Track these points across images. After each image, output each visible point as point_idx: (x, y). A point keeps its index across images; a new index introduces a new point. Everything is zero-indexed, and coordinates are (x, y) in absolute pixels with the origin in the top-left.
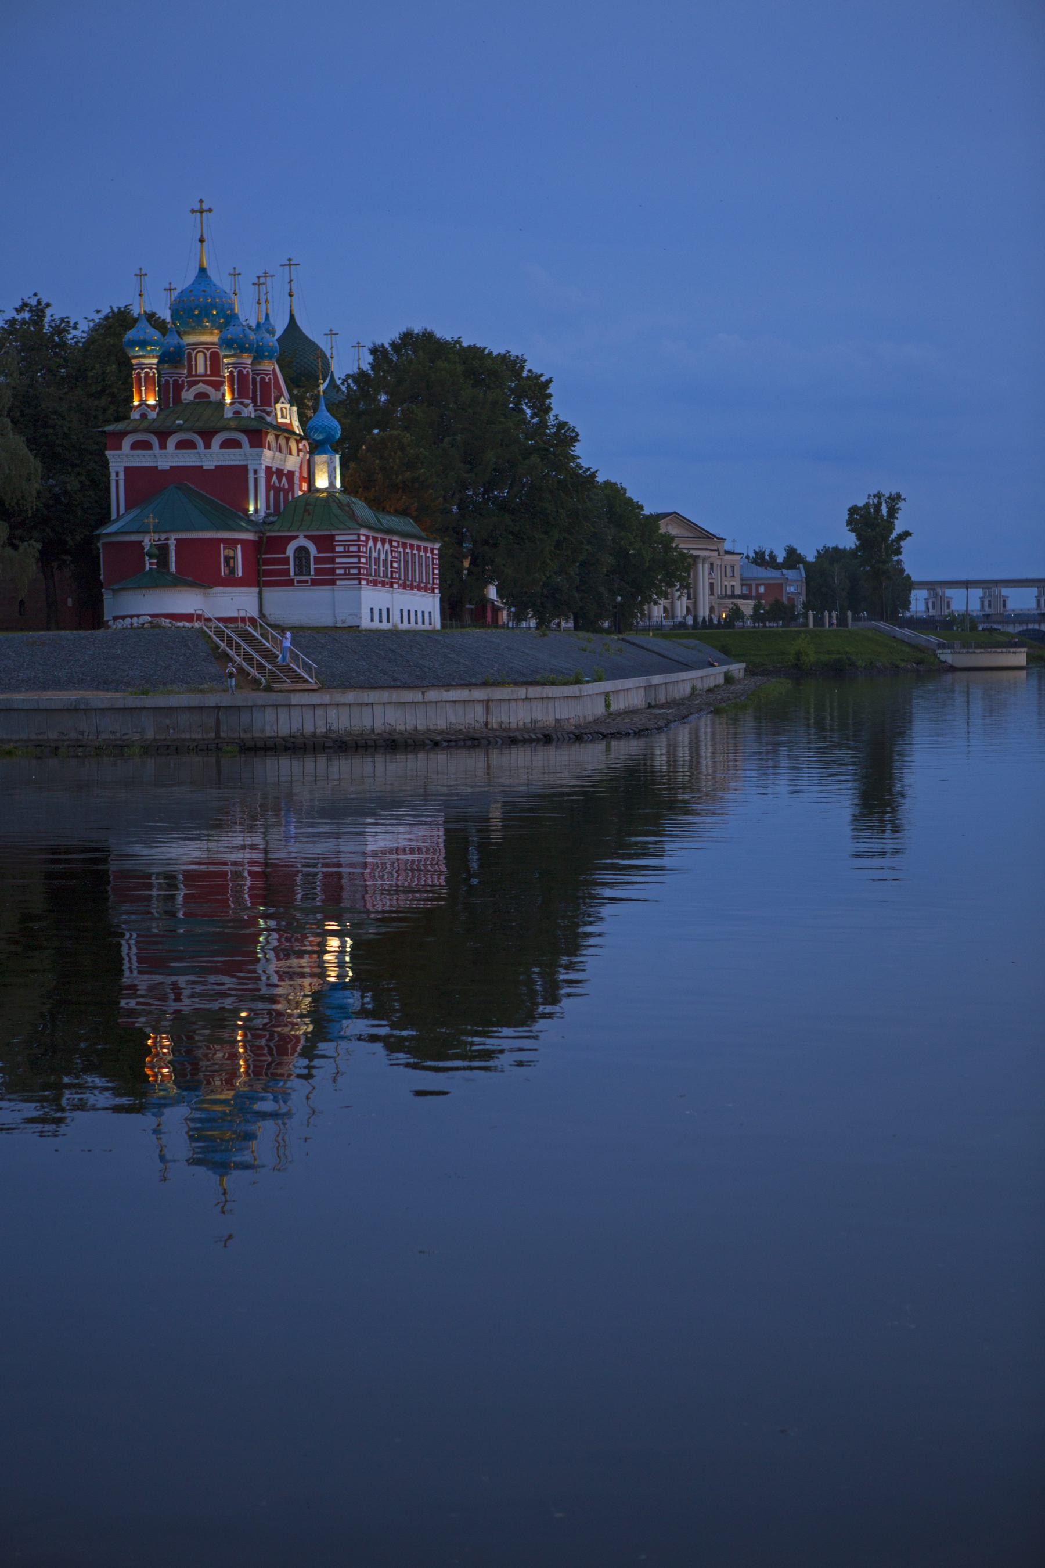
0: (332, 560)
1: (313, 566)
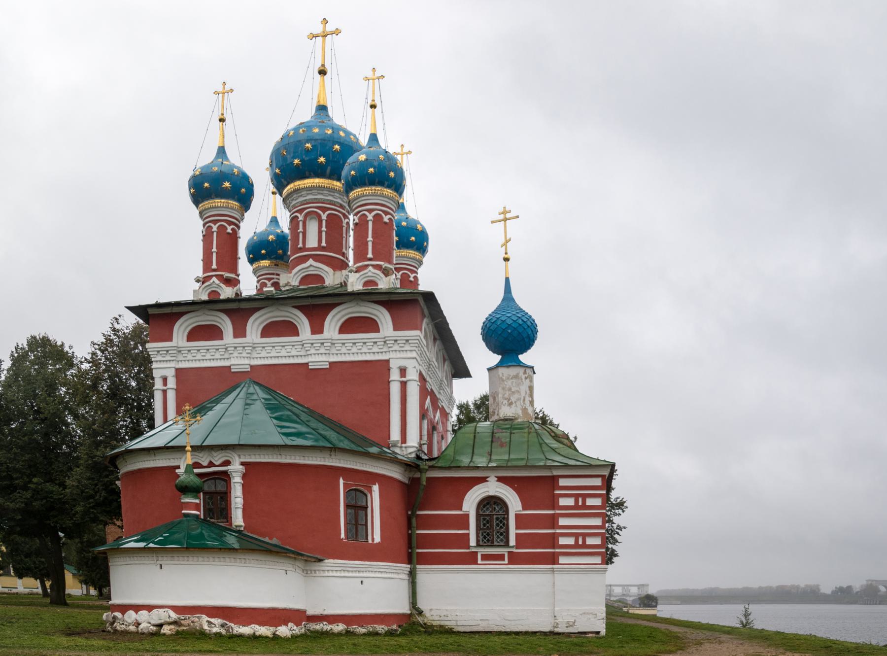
0: (552, 522)
1: (513, 531)
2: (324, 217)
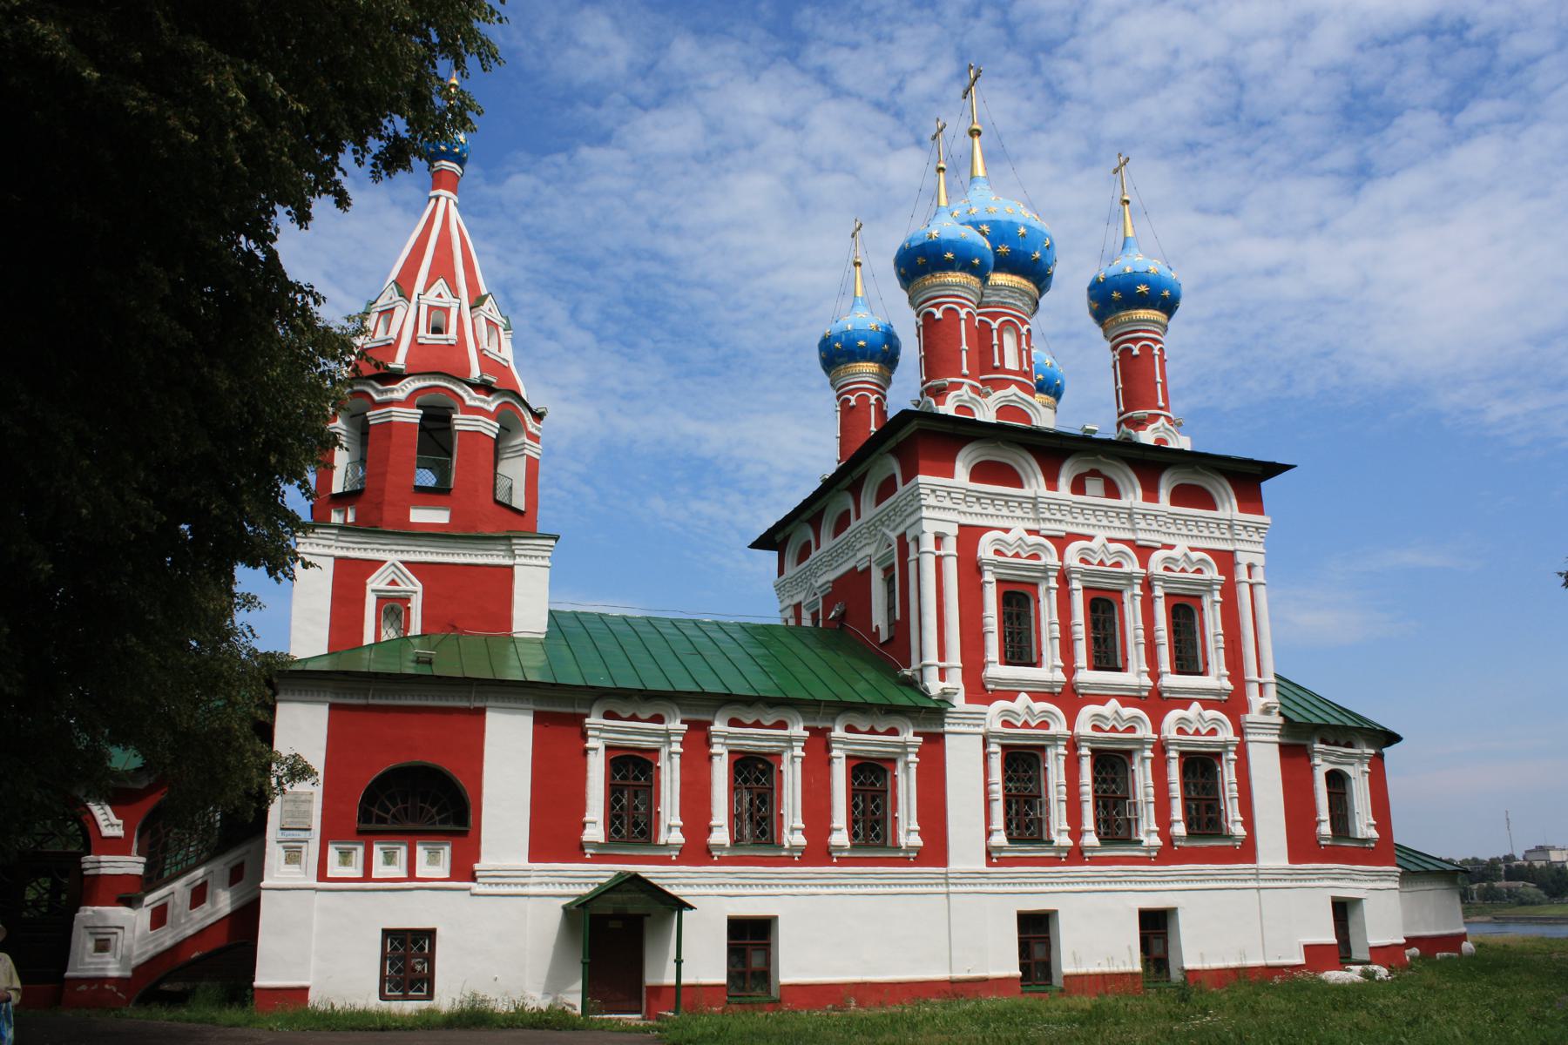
2: (1024, 330)
